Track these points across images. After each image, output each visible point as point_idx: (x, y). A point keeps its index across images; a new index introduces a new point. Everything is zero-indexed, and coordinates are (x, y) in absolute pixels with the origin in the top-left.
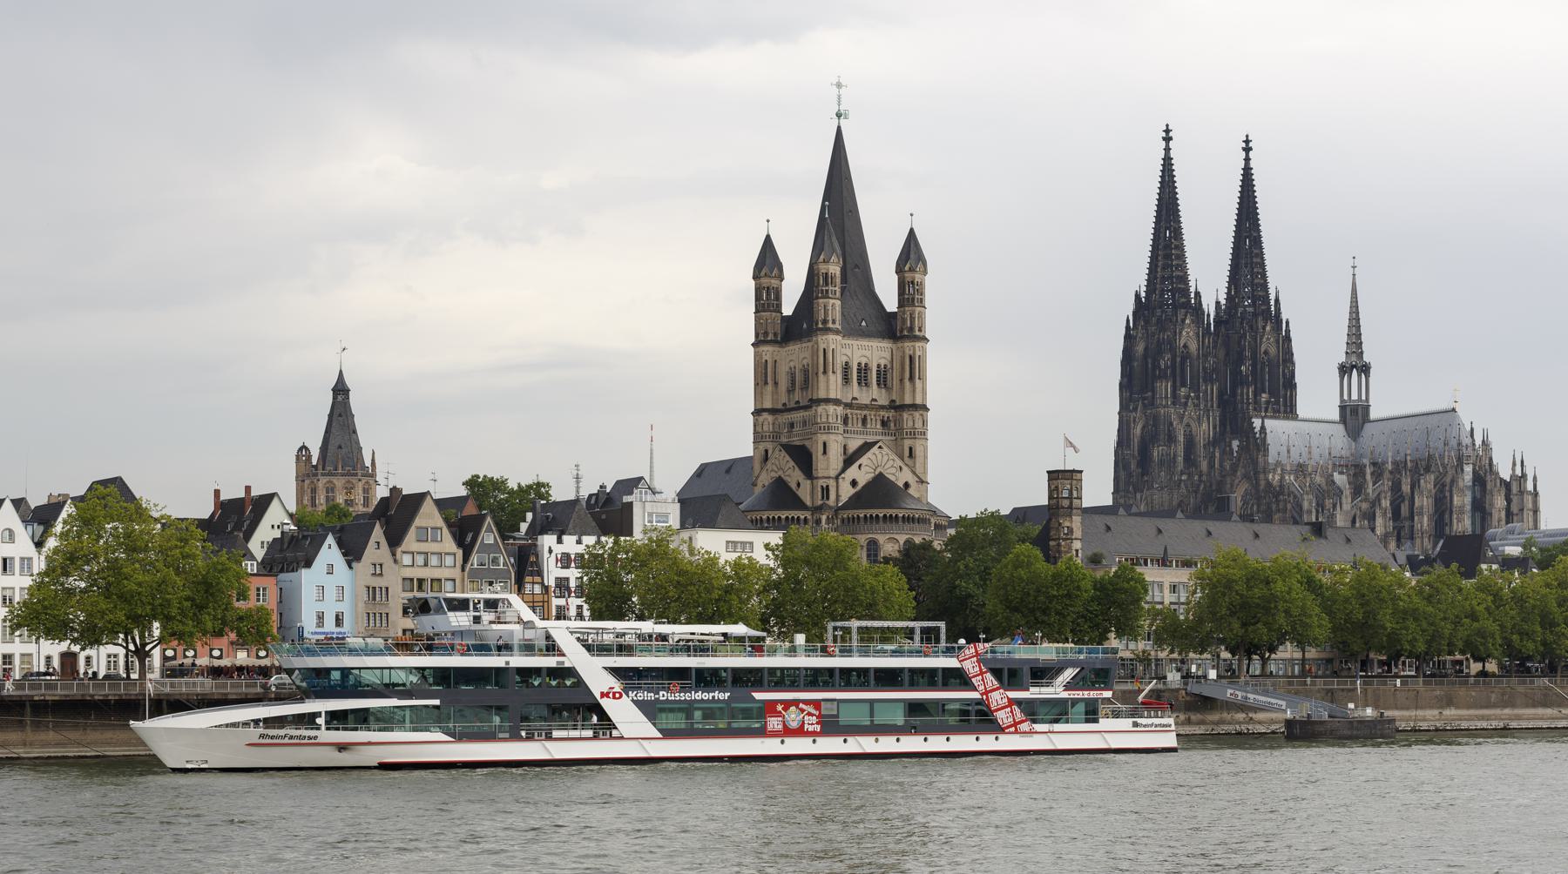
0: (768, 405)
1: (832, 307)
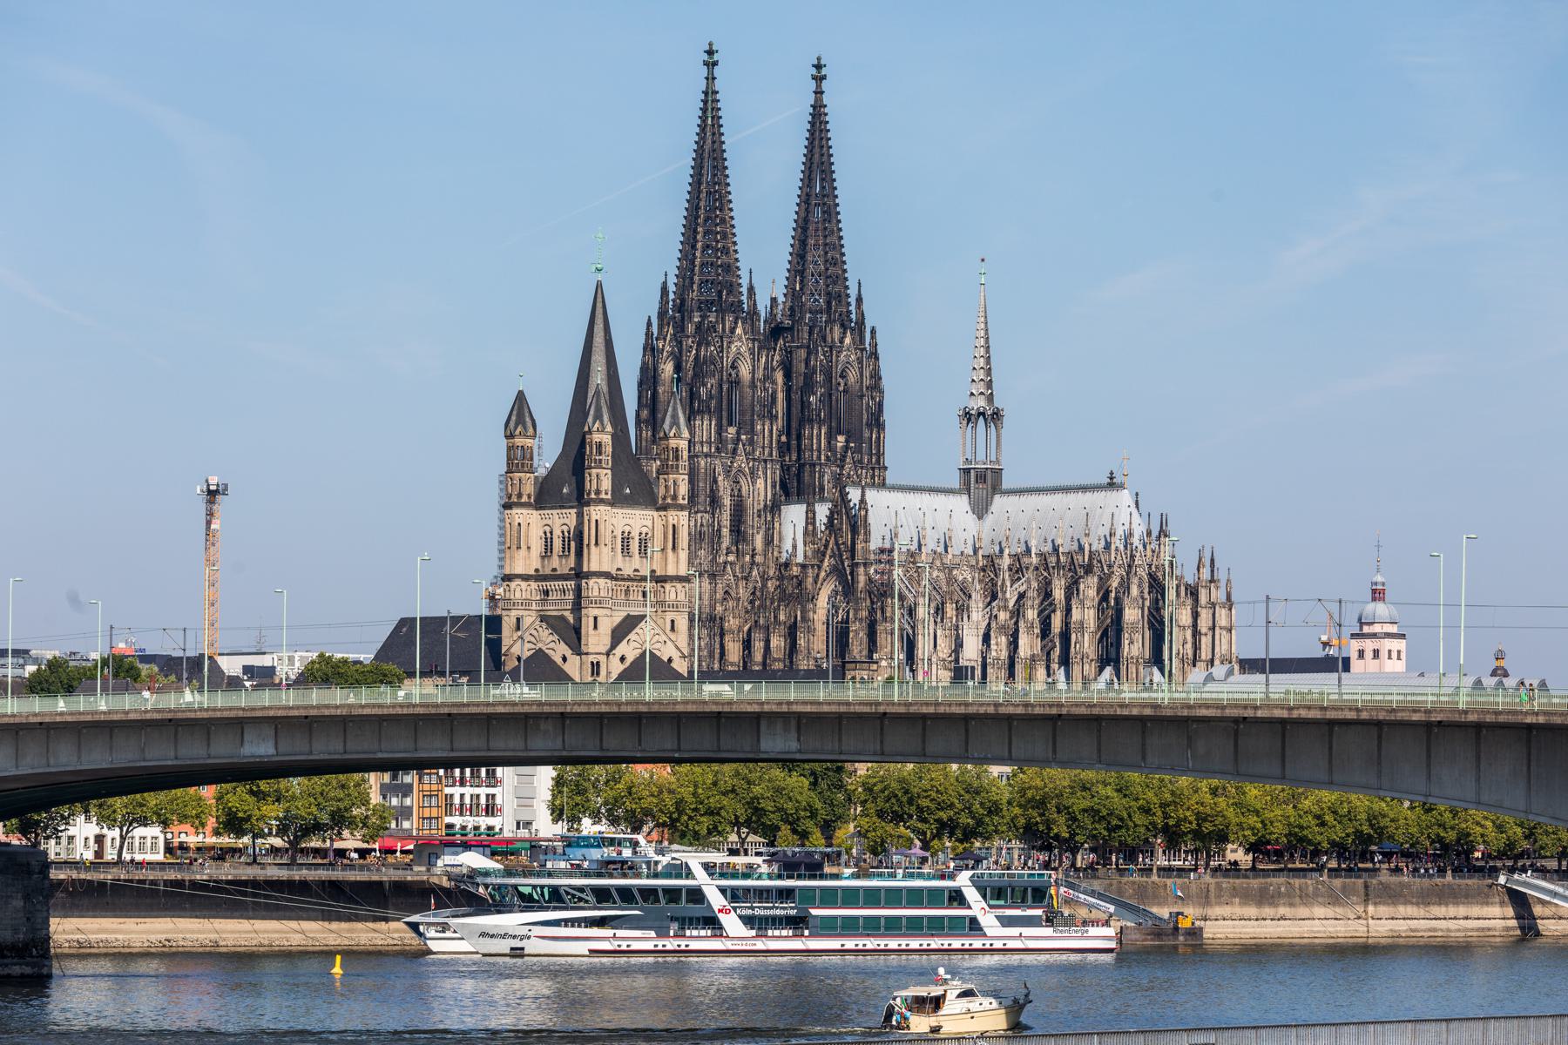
0: (519, 570)
1: (602, 479)
